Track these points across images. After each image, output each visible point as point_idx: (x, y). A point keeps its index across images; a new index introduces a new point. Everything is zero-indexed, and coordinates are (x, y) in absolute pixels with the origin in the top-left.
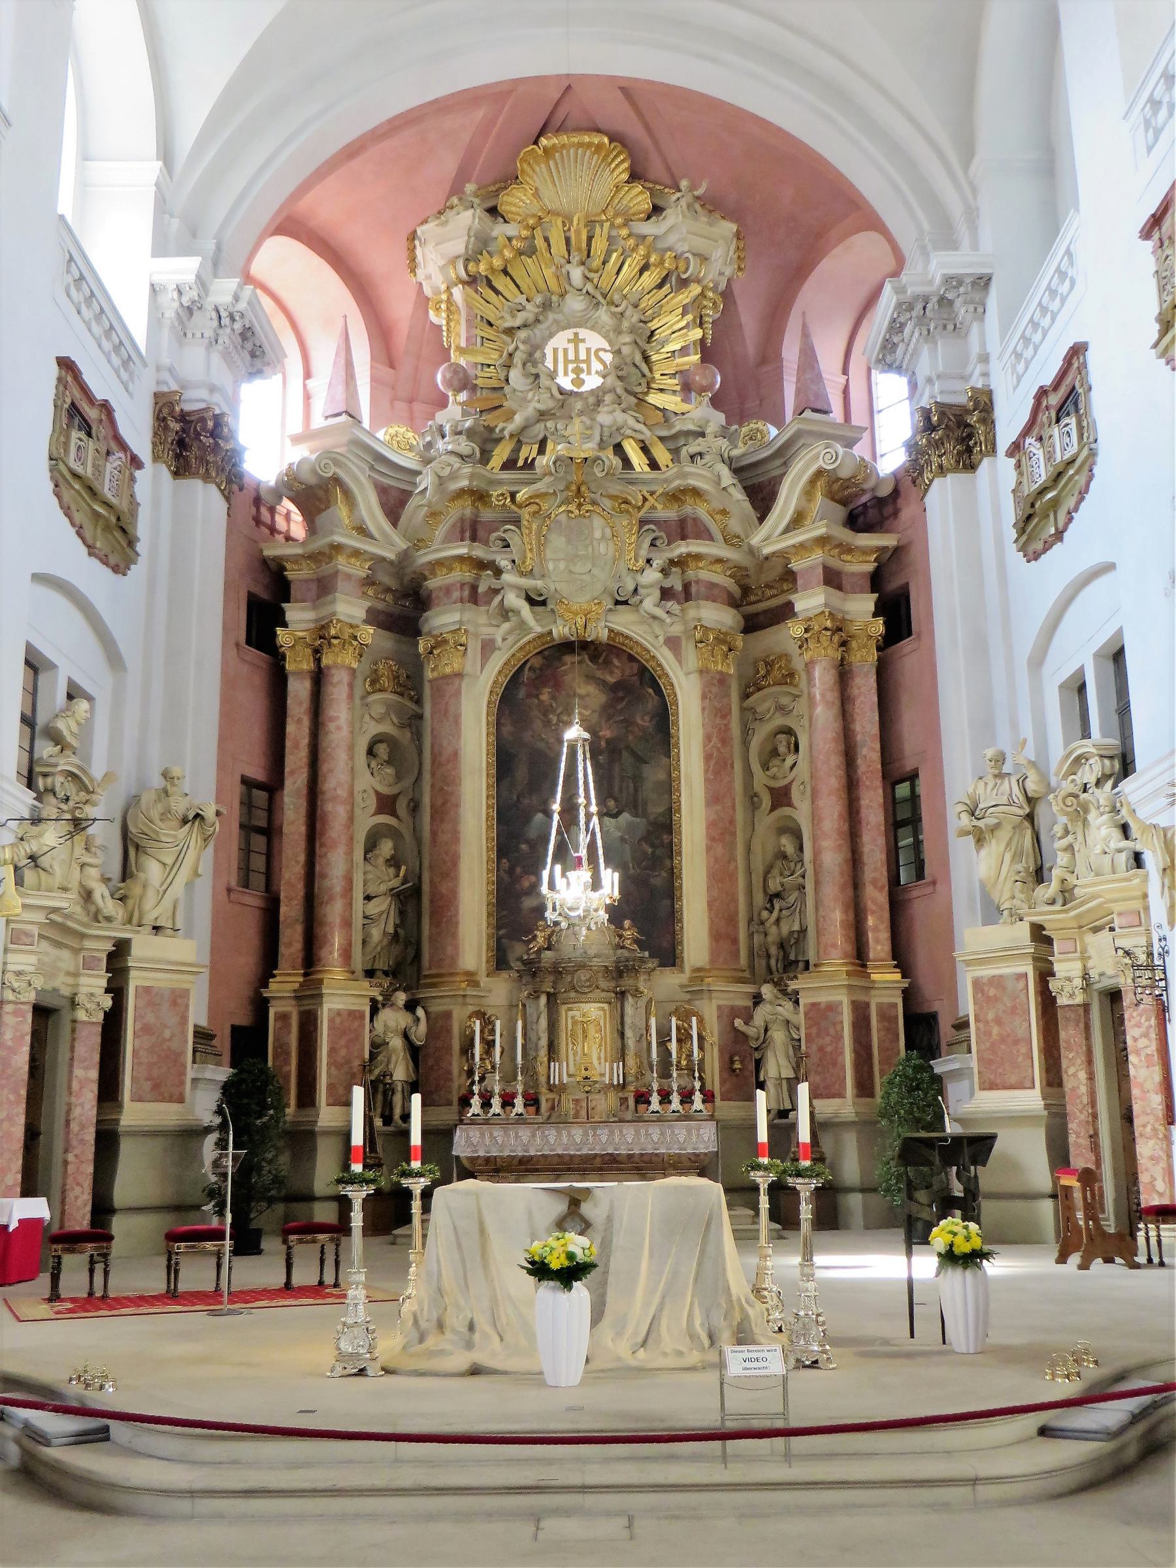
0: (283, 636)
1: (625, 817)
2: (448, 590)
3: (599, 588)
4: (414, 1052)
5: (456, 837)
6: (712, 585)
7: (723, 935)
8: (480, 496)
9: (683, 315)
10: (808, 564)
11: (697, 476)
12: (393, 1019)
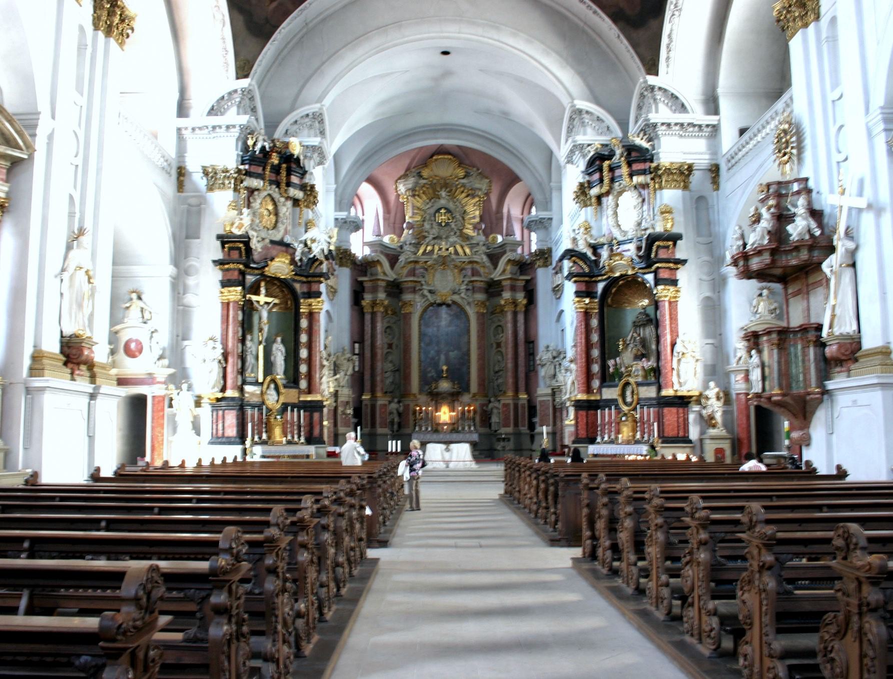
0: (364, 303)
1: (456, 352)
2: (408, 288)
3: (448, 289)
4: (400, 414)
5: (410, 357)
6: (480, 288)
7: (482, 383)
8: (416, 262)
9: (474, 206)
10: (506, 283)
11: (476, 258)
12: (394, 406)
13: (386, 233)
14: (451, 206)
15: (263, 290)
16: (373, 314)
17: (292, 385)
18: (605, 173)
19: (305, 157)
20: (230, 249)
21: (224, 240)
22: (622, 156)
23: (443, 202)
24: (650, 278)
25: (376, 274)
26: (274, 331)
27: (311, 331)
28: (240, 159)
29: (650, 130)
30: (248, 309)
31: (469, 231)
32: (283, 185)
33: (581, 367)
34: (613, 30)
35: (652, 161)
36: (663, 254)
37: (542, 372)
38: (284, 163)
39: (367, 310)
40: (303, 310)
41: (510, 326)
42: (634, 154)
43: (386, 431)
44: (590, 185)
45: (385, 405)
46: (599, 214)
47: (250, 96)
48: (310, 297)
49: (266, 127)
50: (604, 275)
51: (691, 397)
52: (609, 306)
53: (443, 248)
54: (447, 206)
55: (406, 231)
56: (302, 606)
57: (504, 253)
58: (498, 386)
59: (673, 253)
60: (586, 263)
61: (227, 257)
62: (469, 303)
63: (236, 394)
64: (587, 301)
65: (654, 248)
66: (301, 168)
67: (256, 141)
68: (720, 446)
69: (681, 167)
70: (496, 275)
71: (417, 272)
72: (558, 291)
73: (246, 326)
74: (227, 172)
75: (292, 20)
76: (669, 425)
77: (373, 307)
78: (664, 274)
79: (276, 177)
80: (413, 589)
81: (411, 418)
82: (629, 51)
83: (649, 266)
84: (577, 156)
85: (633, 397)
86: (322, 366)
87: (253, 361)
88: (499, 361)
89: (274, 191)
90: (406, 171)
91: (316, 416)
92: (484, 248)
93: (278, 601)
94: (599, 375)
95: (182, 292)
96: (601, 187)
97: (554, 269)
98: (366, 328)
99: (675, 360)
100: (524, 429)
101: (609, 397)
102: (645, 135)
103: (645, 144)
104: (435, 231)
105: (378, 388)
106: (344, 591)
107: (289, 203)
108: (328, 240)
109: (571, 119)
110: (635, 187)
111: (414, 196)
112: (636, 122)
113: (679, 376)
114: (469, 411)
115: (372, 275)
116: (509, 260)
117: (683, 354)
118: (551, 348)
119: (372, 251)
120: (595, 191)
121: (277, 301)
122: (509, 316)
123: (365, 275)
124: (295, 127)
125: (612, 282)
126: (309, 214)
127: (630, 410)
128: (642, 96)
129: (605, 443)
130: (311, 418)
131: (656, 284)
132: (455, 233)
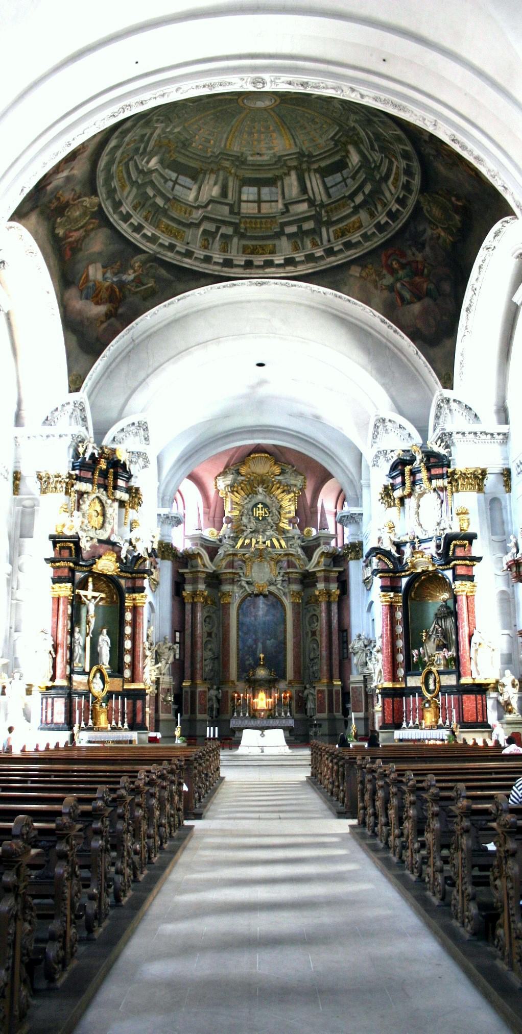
0: (184, 594)
2: (226, 580)
4: (218, 701)
5: (229, 646)
7: (297, 671)
8: (234, 555)
11: (292, 551)
12: (213, 692)
13: (206, 527)
14: (268, 501)
15: (90, 585)
16: (194, 605)
17: (117, 674)
18: (407, 477)
19: (131, 462)
20: (61, 548)
21: (55, 540)
22: (422, 461)
23: (260, 497)
24: (449, 574)
25: (197, 566)
26: (100, 624)
27: (134, 624)
28: (71, 465)
29: (445, 438)
30: (77, 603)
31: (285, 525)
32: (111, 488)
33: (387, 657)
34: (412, 348)
35: (449, 467)
36: (460, 552)
37: (355, 660)
38: (111, 468)
39: (188, 600)
40: (128, 603)
41: (324, 615)
42: (432, 460)
43: (205, 716)
44: (393, 487)
45: (205, 692)
46: (402, 514)
47: (81, 408)
48: (134, 592)
49: (95, 433)
50: (407, 571)
51: (488, 684)
52: (412, 599)
53: (259, 541)
54: (264, 502)
55: (225, 525)
56: (138, 846)
57: (319, 545)
58: (313, 673)
59: (469, 550)
60: (390, 560)
61: (58, 556)
62: (284, 594)
63: (64, 683)
64: (392, 594)
65: (452, 546)
66: (127, 472)
67: (86, 448)
68: (517, 730)
69: (475, 471)
70: (311, 567)
71: (235, 564)
72: (367, 582)
73: (75, 620)
74: (59, 476)
75: (120, 338)
76: (469, 711)
77: (193, 598)
78: (461, 571)
79: (104, 481)
80: (219, 847)
81: (230, 703)
82: (426, 366)
83: (448, 563)
84: (382, 459)
85: (435, 685)
86: (145, 657)
87: (81, 652)
88: (314, 649)
89: (102, 494)
90: (225, 468)
91: (139, 703)
92: (299, 541)
93: (125, 836)
94: (404, 664)
95: (15, 587)
96: (403, 490)
97: (364, 562)
98: (186, 617)
99: (473, 650)
100: (339, 715)
101: (414, 685)
102: (442, 442)
103: (443, 451)
104: (253, 525)
105: (198, 676)
106: (165, 846)
107: (116, 505)
108: (153, 540)
109: (376, 427)
110: (435, 490)
111: (232, 492)
112: (435, 430)
113: (476, 664)
114: (285, 698)
115: (192, 566)
116: (323, 553)
117: (480, 644)
118: (362, 637)
119: (193, 545)
120: (398, 493)
121: (103, 595)
122: (323, 606)
123: (187, 568)
124: (122, 434)
125: (415, 577)
126: (132, 514)
127: (432, 698)
128: (439, 407)
129: (410, 728)
130: (134, 705)
131: (454, 580)
132: (272, 527)
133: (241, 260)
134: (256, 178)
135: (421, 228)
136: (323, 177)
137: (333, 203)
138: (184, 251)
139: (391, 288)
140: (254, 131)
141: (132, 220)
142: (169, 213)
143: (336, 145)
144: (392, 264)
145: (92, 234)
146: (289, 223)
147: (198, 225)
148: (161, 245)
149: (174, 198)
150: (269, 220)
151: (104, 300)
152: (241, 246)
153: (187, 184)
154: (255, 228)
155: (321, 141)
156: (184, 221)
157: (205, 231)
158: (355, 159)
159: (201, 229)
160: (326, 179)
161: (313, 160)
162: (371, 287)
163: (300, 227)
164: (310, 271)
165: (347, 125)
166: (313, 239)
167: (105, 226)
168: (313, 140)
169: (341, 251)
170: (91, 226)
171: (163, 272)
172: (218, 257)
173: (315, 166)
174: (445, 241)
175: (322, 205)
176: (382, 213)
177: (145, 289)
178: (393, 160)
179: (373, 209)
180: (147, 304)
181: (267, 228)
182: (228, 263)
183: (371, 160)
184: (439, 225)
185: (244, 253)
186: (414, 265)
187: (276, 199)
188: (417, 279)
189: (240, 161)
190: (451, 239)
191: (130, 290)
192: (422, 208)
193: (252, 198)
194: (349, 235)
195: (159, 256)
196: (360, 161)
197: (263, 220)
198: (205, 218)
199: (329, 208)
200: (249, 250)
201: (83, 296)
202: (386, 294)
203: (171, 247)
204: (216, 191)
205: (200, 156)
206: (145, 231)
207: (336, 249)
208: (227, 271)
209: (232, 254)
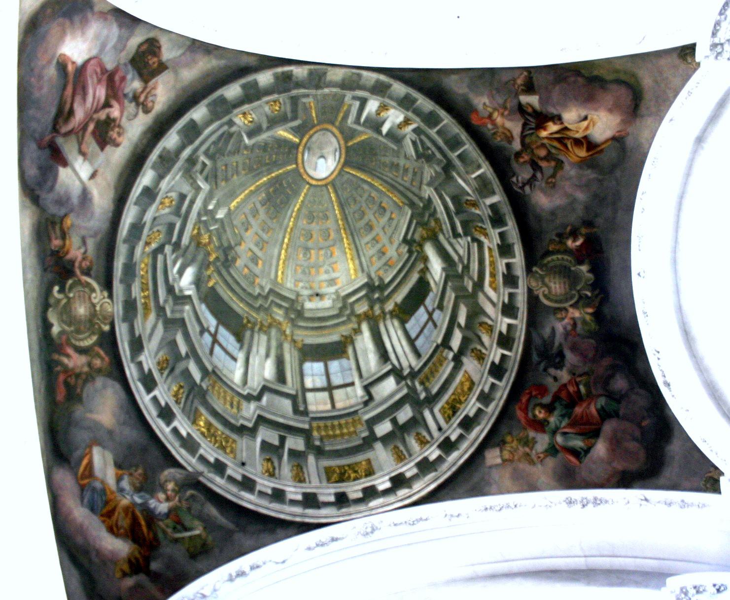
133: (327, 494)
134: (319, 346)
135: (547, 332)
136: (403, 322)
137: (425, 364)
138: (239, 478)
139: (553, 450)
140: (310, 244)
141: (156, 392)
142: (208, 398)
143: (410, 252)
144: (535, 416)
145: (99, 382)
146: (379, 418)
147: (252, 432)
148: (202, 459)
149: (214, 372)
150: (350, 420)
151: (122, 531)
152: (322, 471)
153: (230, 349)
154: (335, 436)
155: (391, 252)
156: (233, 421)
157: (265, 446)
158: (436, 266)
159: (259, 440)
160: (408, 326)
161: (386, 293)
162: (524, 466)
163: (394, 421)
164: (433, 486)
165: (421, 198)
166: (418, 434)
167: (115, 379)
168: (382, 253)
169: (461, 437)
170: (97, 362)
171: (213, 511)
172: (294, 492)
173: (390, 306)
174: (584, 322)
175: (413, 374)
176: (491, 346)
177: (191, 537)
178: (482, 238)
179: (479, 347)
180: (199, 566)
181: (350, 434)
182: (310, 500)
183: (456, 258)
184: (566, 305)
185: (329, 480)
186: (563, 394)
187: (349, 381)
188: (578, 410)
189: (295, 311)
190: (590, 310)
191: (164, 532)
192: (537, 298)
193: (321, 382)
194: (463, 406)
195: (201, 479)
196: (444, 269)
197: (343, 421)
198: (261, 420)
199: (422, 375)
200: (335, 477)
201: (86, 500)
202: (550, 462)
203: (219, 467)
204: (269, 371)
205: (244, 290)
206: (175, 423)
207: (453, 438)
208: (311, 515)
209: (313, 484)
